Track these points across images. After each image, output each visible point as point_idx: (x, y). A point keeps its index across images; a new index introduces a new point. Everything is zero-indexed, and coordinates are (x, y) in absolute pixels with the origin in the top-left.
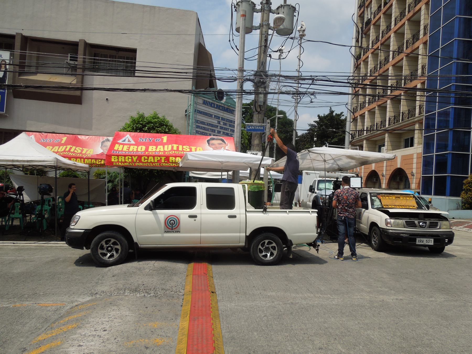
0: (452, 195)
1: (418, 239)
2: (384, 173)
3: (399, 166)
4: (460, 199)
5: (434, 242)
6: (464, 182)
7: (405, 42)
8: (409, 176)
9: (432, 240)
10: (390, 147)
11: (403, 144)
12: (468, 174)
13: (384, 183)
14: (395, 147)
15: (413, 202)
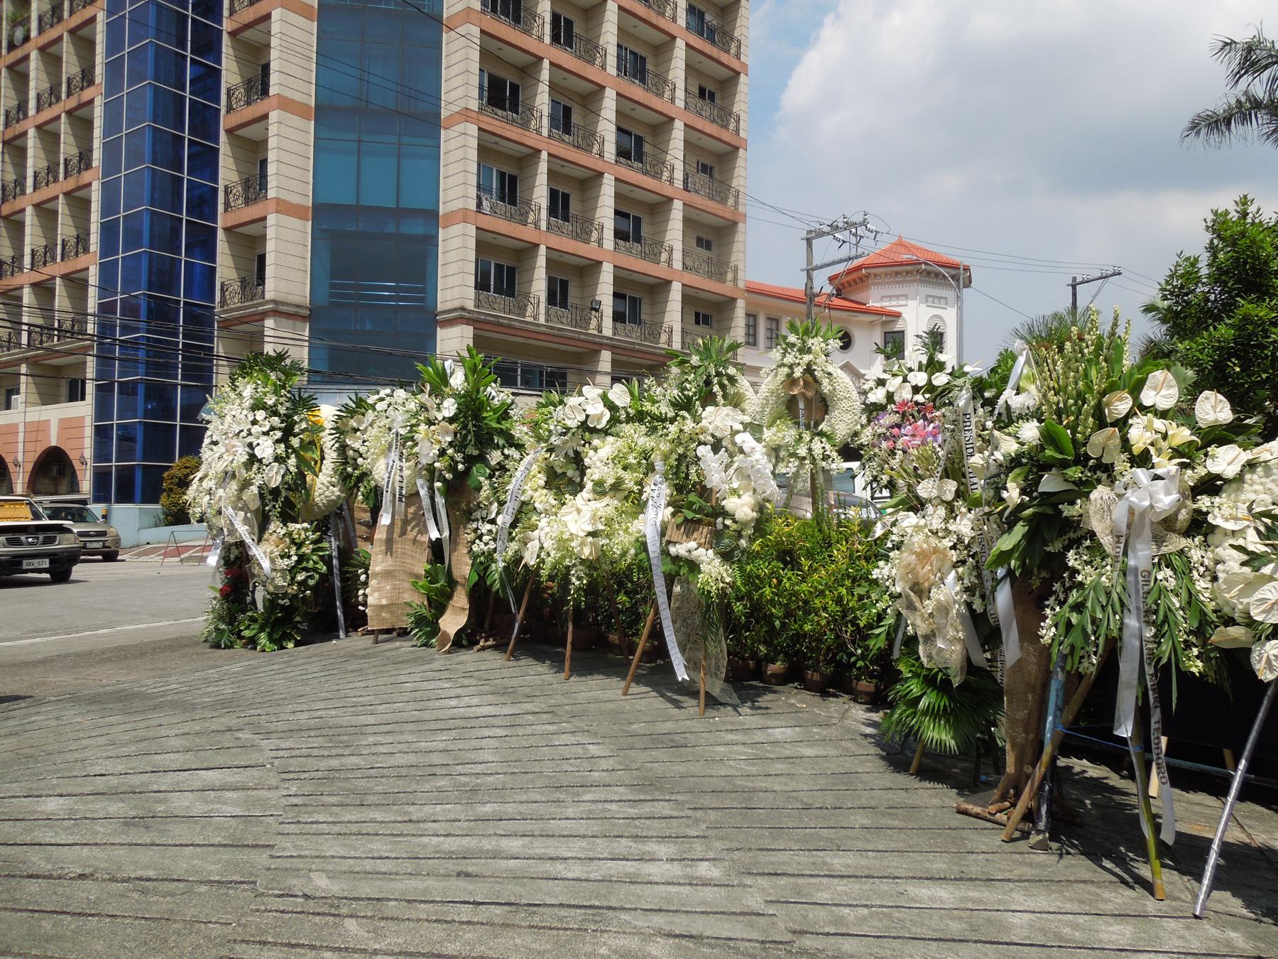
0: (145, 500)
1: (25, 562)
2: (20, 459)
3: (53, 443)
4: (158, 506)
5: (50, 563)
6: (165, 475)
7: (62, 161)
8: (77, 465)
9: (47, 560)
10: (36, 398)
11: (64, 390)
12: (173, 460)
13: (20, 481)
14: (48, 398)
15: (27, 511)
